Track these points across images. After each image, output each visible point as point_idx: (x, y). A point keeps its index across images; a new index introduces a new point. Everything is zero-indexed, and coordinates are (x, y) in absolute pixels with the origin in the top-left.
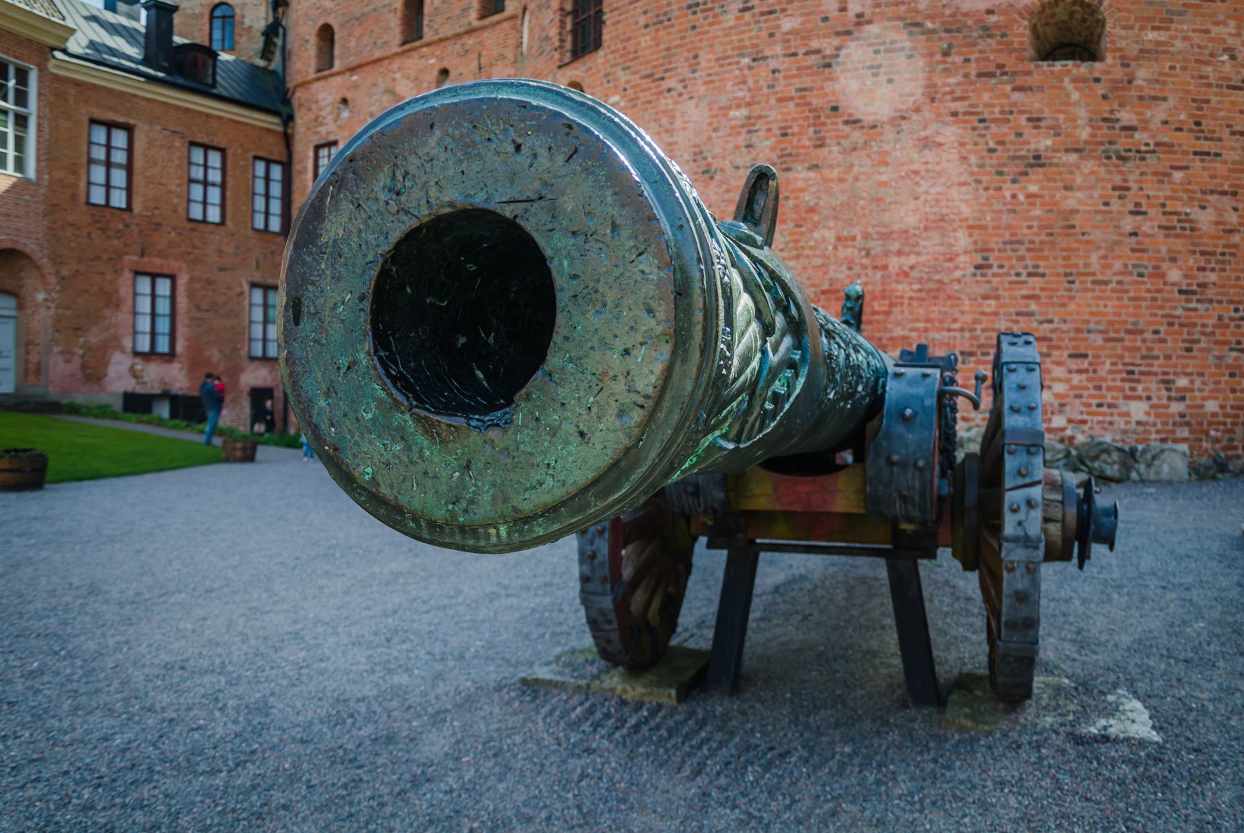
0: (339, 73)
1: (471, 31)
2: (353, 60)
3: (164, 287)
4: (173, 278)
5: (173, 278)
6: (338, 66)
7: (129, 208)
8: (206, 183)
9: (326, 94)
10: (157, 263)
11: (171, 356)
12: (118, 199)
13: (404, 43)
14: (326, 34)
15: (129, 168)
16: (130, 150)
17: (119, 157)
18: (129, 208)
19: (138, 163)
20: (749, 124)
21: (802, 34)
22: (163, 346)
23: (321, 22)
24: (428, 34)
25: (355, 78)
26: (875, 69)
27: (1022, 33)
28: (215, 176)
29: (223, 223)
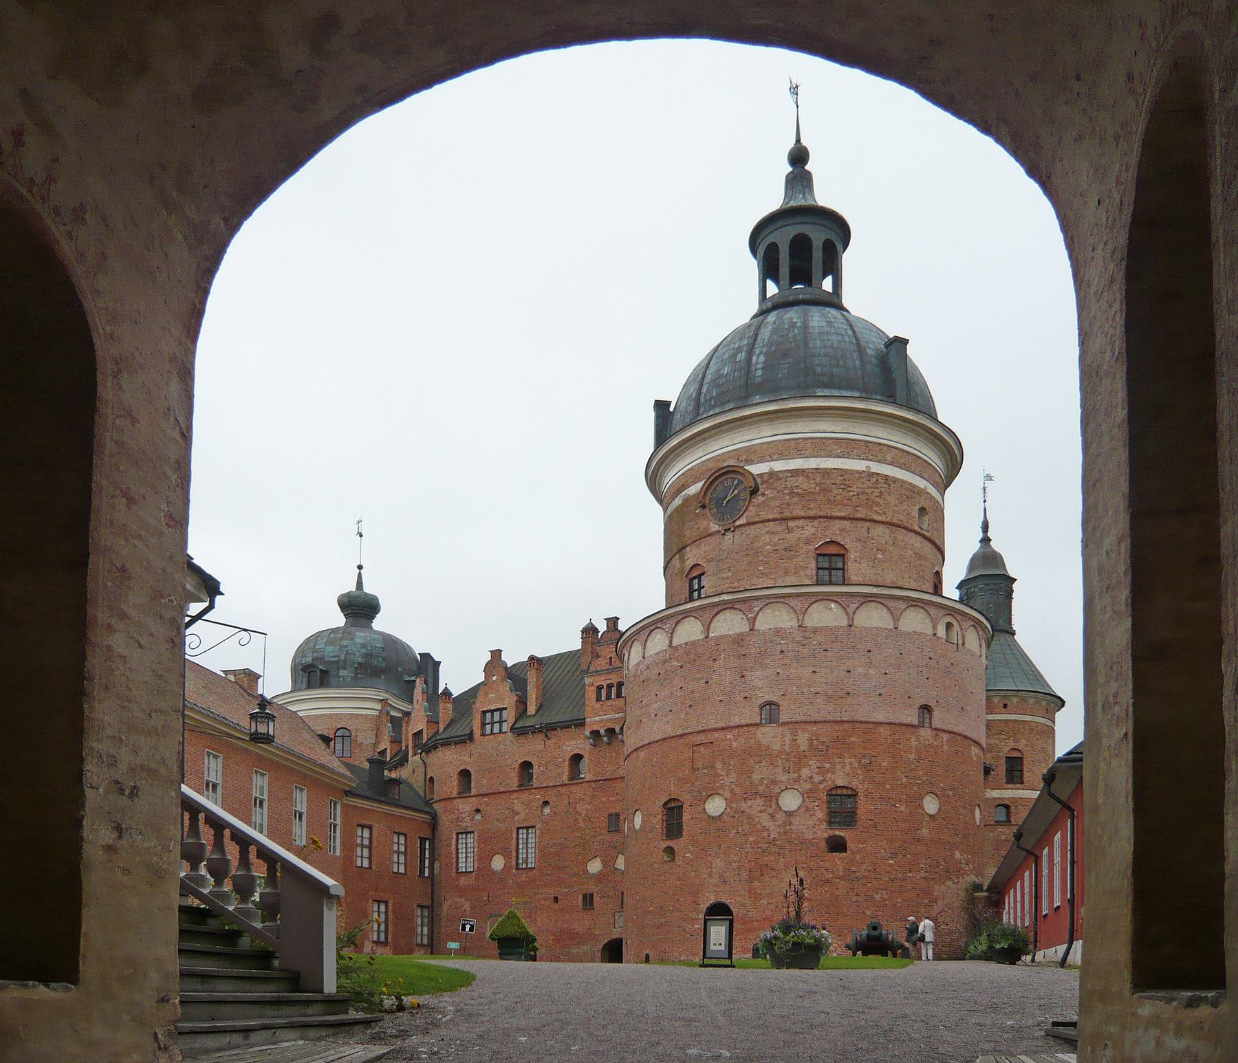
2: (484, 791)
3: (383, 908)
4: (386, 903)
5: (386, 903)
6: (473, 792)
7: (370, 867)
8: (399, 853)
9: (465, 806)
10: (381, 896)
11: (385, 944)
12: (366, 864)
14: (465, 775)
15: (370, 847)
16: (371, 838)
17: (366, 842)
18: (370, 867)
19: (374, 845)
20: (739, 868)
21: (757, 842)
22: (382, 938)
24: (535, 783)
26: (779, 854)
27: (823, 844)
28: (402, 849)
29: (406, 873)
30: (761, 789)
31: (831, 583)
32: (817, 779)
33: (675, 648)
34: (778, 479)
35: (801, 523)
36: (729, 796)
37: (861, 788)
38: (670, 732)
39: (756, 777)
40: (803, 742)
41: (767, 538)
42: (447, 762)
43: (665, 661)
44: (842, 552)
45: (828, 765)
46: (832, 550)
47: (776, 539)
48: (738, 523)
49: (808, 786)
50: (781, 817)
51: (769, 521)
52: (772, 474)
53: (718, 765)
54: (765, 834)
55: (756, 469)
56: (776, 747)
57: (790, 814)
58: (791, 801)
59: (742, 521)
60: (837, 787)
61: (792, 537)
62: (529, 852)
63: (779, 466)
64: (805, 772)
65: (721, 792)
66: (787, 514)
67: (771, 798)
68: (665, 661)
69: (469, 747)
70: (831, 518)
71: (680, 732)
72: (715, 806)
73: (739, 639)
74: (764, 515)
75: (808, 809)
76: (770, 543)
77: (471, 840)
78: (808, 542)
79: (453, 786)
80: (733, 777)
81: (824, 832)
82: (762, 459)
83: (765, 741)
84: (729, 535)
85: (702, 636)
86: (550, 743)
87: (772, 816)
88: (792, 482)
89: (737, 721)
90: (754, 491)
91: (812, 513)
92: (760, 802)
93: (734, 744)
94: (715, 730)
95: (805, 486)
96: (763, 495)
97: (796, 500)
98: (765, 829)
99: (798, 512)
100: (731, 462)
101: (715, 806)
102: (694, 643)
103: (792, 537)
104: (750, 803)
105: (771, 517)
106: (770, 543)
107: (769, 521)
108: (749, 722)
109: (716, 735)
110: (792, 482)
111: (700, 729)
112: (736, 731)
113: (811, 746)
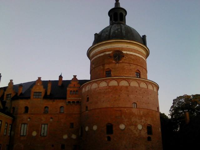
0: (29, 114)
1: (58, 114)
6: (29, 113)
9: (25, 117)
13: (44, 113)
23: (26, 106)
25: (32, 115)
29: (6, 135)
30: (134, 123)
31: (137, 77)
32: (145, 122)
33: (110, 86)
34: (128, 55)
35: (132, 65)
36: (126, 124)
37: (152, 125)
38: (108, 106)
39: (133, 120)
40: (141, 113)
41: (126, 66)
42: (22, 103)
43: (107, 89)
44: (139, 72)
45: (146, 119)
46: (138, 71)
47: (128, 67)
48: (120, 62)
49: (143, 124)
50: (138, 131)
51: (127, 63)
52: (127, 54)
53: (123, 116)
54: (135, 135)
55: (124, 52)
56: (136, 113)
57: (140, 130)
58: (140, 127)
59: (121, 62)
60: (149, 125)
61: (132, 67)
62: (45, 129)
63: (128, 53)
64: (143, 120)
65: (124, 123)
66: (130, 63)
67: (136, 126)
68: (107, 89)
69: (29, 100)
70: (138, 65)
71: (112, 106)
72: (122, 127)
73: (127, 87)
74: (125, 61)
75: (144, 130)
76: (127, 67)
77: (26, 126)
78: (134, 69)
79: (23, 110)
80: (126, 120)
81: (147, 136)
82: (125, 51)
83: (134, 112)
84: (117, 64)
85: (117, 85)
86: (55, 103)
87: (137, 131)
88: (131, 56)
89: (127, 106)
90: (124, 56)
91: (135, 63)
92: (134, 127)
93: (127, 111)
94: (122, 107)
95: (133, 58)
96: (125, 57)
97: (132, 60)
98: (135, 134)
99: (132, 62)
100: (118, 49)
101: (122, 127)
102: (115, 86)
103: (132, 67)
104: (131, 127)
105: (127, 62)
106: (127, 67)
107: (127, 63)
108: (130, 107)
109: (122, 109)
110: (131, 56)
111: (118, 106)
112: (127, 109)
113: (143, 114)
